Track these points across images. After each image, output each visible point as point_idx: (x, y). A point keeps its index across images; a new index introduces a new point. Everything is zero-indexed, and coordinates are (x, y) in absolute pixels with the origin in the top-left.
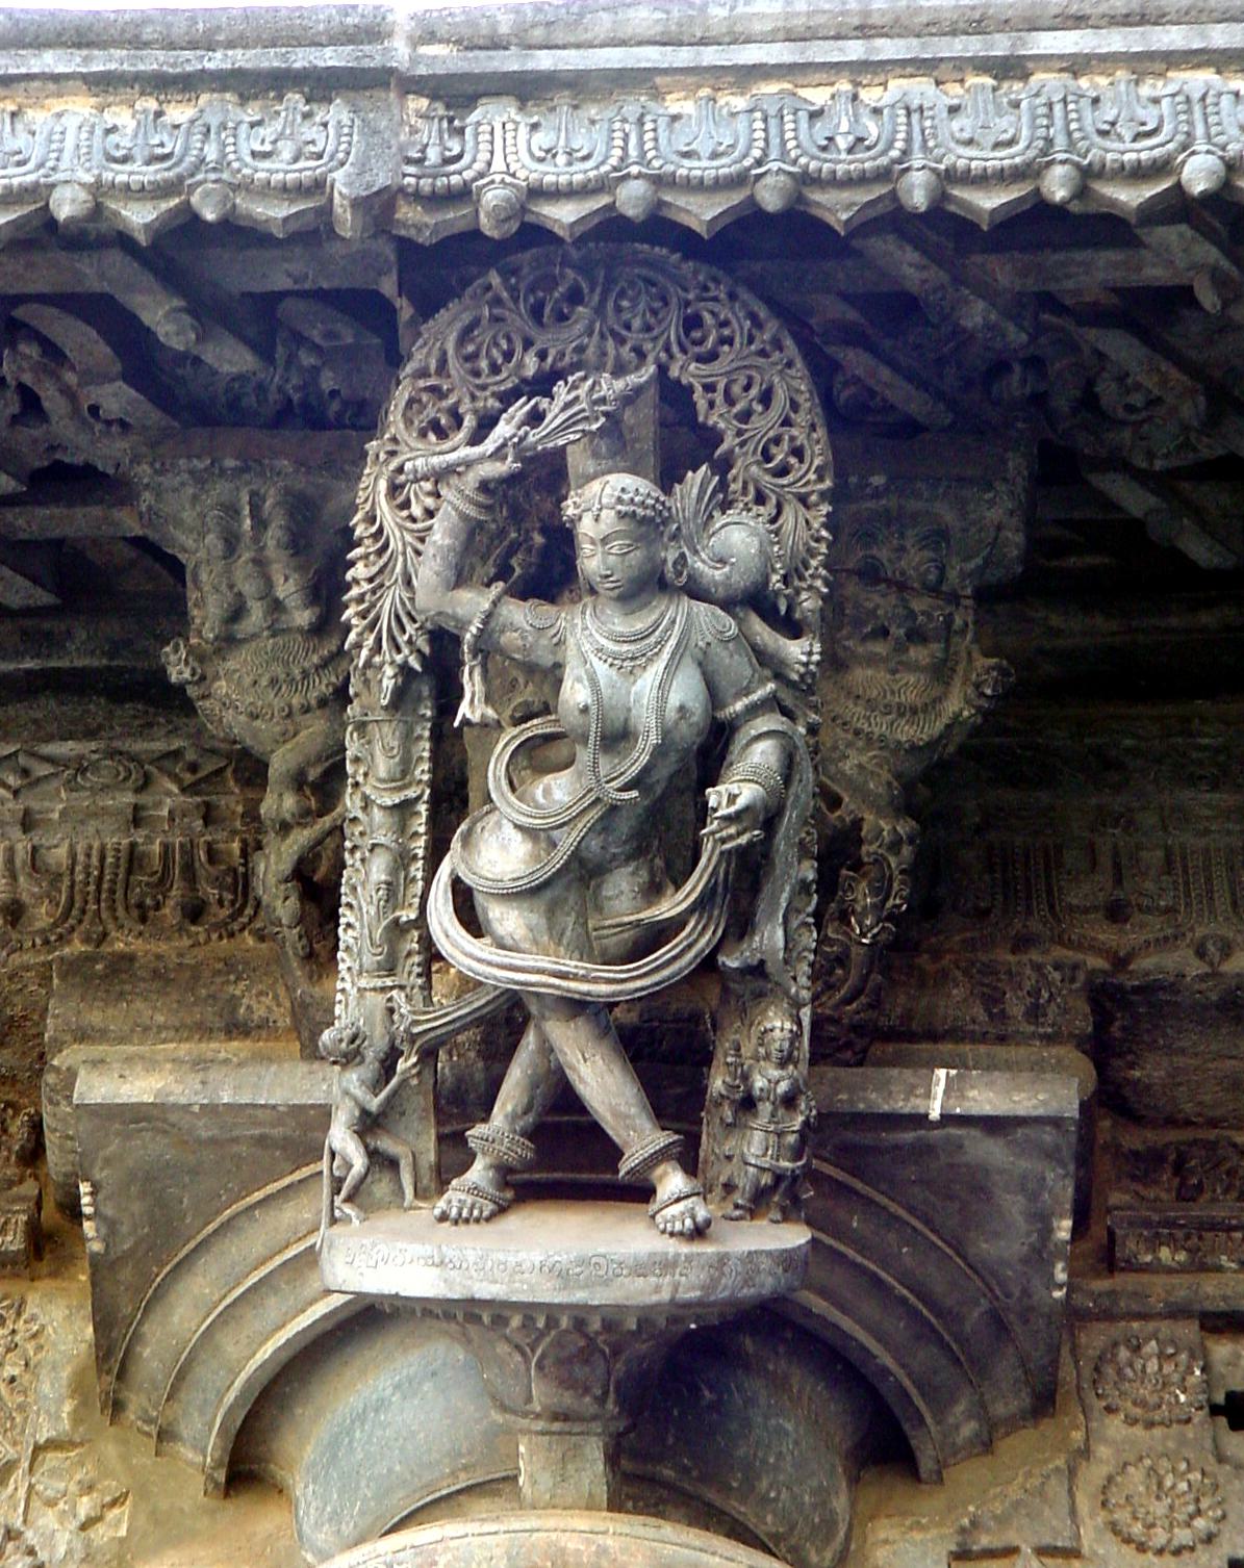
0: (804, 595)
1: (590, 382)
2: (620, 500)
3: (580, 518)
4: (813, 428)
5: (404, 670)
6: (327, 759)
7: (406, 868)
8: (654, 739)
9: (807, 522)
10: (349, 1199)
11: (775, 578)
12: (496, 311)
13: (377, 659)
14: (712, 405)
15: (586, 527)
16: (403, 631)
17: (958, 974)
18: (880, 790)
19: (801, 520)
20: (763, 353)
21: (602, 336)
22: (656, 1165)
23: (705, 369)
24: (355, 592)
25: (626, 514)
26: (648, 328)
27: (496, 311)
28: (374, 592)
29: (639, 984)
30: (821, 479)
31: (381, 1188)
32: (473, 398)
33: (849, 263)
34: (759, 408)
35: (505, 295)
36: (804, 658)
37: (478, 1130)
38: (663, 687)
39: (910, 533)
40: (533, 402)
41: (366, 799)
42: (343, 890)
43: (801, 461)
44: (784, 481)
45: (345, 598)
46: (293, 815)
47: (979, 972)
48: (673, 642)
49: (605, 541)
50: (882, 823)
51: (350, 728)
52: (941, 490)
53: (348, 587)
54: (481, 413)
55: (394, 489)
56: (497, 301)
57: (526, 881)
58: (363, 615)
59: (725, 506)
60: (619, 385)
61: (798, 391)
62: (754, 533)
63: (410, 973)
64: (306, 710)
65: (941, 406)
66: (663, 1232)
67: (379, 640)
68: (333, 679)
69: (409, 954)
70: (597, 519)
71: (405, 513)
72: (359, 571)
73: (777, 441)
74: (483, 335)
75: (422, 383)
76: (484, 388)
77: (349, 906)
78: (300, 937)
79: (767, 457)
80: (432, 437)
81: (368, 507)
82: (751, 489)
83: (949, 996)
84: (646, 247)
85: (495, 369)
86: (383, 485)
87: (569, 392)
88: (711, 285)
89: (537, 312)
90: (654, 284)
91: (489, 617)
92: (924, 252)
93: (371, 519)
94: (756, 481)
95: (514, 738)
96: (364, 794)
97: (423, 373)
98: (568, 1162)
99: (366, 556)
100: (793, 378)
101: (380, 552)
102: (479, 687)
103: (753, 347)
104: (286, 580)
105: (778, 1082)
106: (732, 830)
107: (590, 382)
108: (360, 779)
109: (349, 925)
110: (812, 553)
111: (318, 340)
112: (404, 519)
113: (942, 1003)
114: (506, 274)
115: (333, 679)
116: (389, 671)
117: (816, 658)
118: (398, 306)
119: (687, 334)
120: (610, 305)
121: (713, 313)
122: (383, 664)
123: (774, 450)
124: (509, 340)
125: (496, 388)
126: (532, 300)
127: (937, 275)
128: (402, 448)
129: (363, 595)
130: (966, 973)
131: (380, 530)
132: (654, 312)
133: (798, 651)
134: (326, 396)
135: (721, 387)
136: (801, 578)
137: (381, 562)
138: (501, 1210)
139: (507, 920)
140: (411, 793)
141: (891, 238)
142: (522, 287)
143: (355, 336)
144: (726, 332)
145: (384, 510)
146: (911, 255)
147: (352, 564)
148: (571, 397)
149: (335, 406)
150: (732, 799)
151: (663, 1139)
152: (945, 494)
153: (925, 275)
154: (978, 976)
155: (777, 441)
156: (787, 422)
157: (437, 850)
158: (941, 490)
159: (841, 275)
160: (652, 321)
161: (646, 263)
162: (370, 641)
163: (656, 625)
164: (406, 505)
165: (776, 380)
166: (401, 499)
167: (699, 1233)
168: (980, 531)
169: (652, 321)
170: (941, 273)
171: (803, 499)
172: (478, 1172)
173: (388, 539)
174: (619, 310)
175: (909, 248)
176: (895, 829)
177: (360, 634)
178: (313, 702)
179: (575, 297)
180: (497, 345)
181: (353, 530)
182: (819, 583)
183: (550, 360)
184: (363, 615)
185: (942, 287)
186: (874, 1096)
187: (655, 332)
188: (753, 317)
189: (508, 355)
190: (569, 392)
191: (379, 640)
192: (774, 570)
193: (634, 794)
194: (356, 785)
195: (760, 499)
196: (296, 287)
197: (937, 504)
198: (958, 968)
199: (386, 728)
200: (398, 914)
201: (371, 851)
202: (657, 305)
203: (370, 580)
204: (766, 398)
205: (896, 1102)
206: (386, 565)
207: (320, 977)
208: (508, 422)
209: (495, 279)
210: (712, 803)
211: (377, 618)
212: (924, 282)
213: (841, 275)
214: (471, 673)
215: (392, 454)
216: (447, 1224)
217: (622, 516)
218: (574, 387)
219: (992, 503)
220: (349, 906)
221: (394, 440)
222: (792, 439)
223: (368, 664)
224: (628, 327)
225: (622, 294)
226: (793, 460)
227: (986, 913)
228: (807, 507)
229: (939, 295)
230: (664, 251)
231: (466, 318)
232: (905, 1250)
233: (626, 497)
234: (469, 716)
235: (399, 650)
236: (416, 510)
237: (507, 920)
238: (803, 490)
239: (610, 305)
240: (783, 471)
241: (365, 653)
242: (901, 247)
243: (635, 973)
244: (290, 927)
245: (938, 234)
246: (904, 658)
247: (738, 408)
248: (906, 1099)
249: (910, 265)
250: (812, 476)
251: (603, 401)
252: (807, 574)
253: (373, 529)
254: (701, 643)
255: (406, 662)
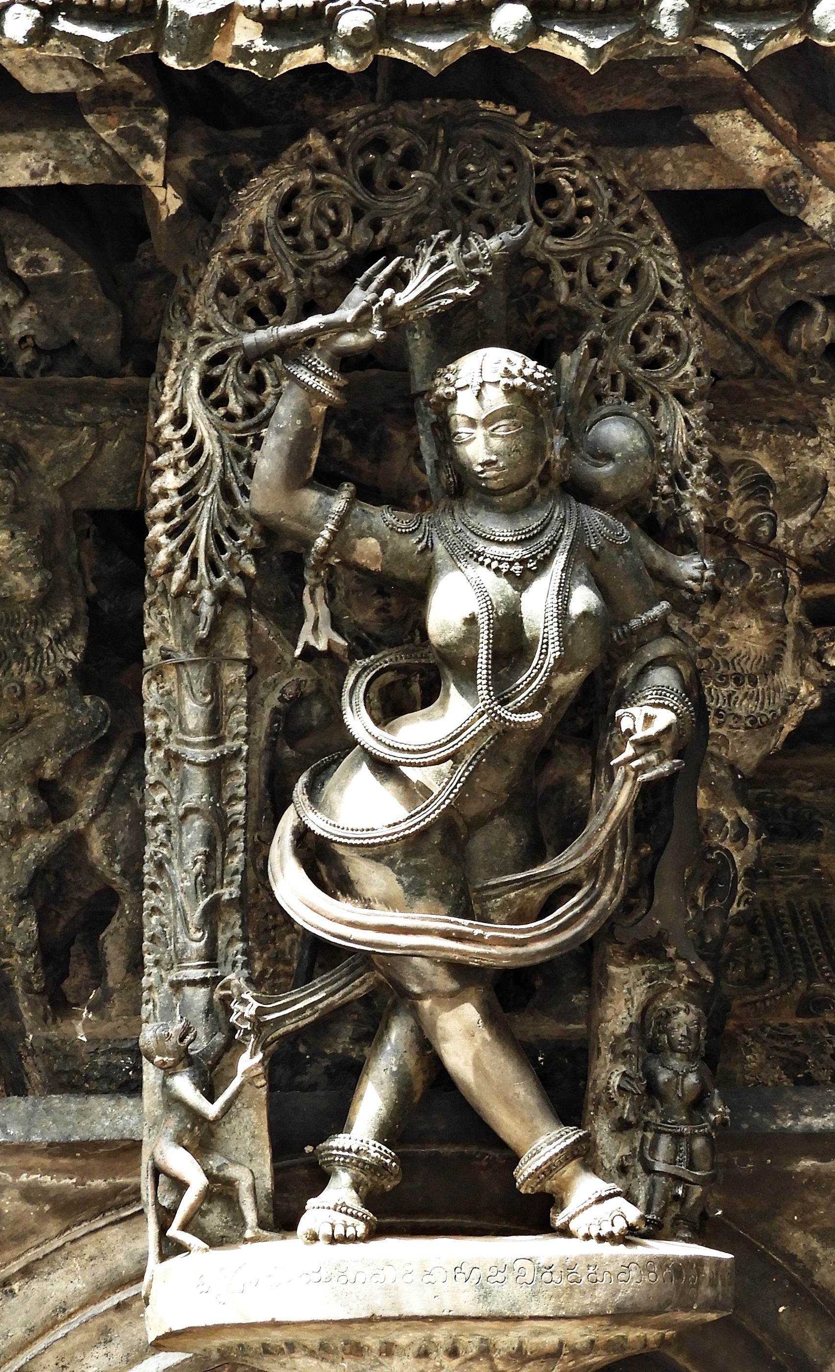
0: (687, 505)
1: (458, 240)
2: (508, 373)
3: (454, 398)
4: (686, 313)
5: (223, 596)
6: (69, 747)
7: (225, 835)
8: (554, 651)
9: (686, 420)
10: (184, 1227)
11: (663, 478)
12: (321, 177)
13: (194, 585)
14: (572, 285)
15: (465, 406)
16: (222, 549)
17: (748, 1039)
18: (723, 773)
19: (680, 418)
20: (627, 227)
21: (445, 207)
22: (567, 1161)
23: (567, 244)
24: (163, 505)
25: (514, 388)
26: (495, 197)
27: (321, 177)
28: (186, 505)
29: (541, 945)
30: (699, 373)
31: (215, 1220)
32: (297, 274)
33: (680, 151)
34: (628, 289)
35: (330, 157)
36: (696, 573)
37: (340, 1141)
38: (564, 594)
39: (733, 480)
40: (393, 263)
41: (174, 759)
42: (146, 869)
43: (677, 352)
44: (660, 373)
45: (153, 512)
46: (30, 815)
47: (770, 1036)
48: (565, 544)
49: (488, 421)
50: (723, 811)
51: (147, 677)
52: (760, 436)
53: (155, 502)
54: (307, 294)
55: (208, 385)
56: (320, 166)
57: (404, 826)
58: (171, 534)
59: (600, 399)
60: (493, 243)
61: (669, 271)
62: (640, 424)
63: (234, 964)
64: (42, 688)
65: (738, 349)
66: (587, 1237)
67: (194, 562)
68: (71, 655)
69: (230, 942)
70: (479, 396)
71: (222, 411)
72: (170, 481)
73: (647, 328)
74: (306, 204)
75: (236, 260)
76: (306, 263)
77: (154, 887)
78: (35, 968)
79: (638, 345)
80: (250, 322)
81: (176, 405)
82: (622, 381)
83: (744, 1061)
84: (490, 106)
85: (322, 243)
86: (195, 378)
87: (433, 254)
88: (567, 148)
89: (366, 177)
90: (500, 147)
91: (343, 519)
92: (774, 134)
93: (179, 420)
94: (626, 371)
95: (365, 669)
96: (168, 752)
97: (235, 251)
98: (447, 1178)
99: (175, 466)
100: (663, 256)
101: (193, 459)
102: (323, 611)
103: (618, 221)
104: (13, 536)
105: (685, 1076)
106: (653, 757)
107: (458, 240)
108: (161, 735)
109: (154, 910)
110: (693, 459)
111: (20, 270)
112: (222, 418)
113: (738, 1068)
114: (330, 136)
115: (71, 655)
116: (207, 595)
117: (707, 574)
118: (160, 197)
119: (541, 206)
120: (453, 169)
121: (573, 182)
122: (200, 588)
123: (645, 338)
124: (337, 212)
125: (323, 263)
126: (361, 163)
127: (785, 158)
128: (216, 334)
129: (173, 508)
130: (755, 1037)
131: (192, 432)
132: (502, 177)
133: (689, 567)
134: (16, 342)
135: (585, 263)
136: (684, 487)
137: (194, 470)
138: (375, 1232)
139: (374, 878)
140: (231, 744)
141: (739, 113)
142: (347, 147)
143: (63, 266)
144: (588, 202)
145: (196, 409)
146: (761, 136)
147: (158, 472)
148: (437, 257)
149: (27, 356)
150: (648, 719)
151: (571, 1135)
152: (766, 440)
153: (773, 160)
154: (769, 1040)
155: (647, 328)
156: (659, 306)
157: (277, 801)
158: (760, 436)
159: (668, 167)
160: (501, 186)
161: (489, 122)
162: (185, 561)
163: (545, 526)
164: (223, 401)
165: (643, 255)
166: (214, 396)
167: (630, 1235)
168: (801, 486)
169: (501, 186)
170: (792, 159)
171: (679, 396)
172: (341, 1190)
173: (201, 444)
174: (463, 174)
175: (758, 127)
176: (739, 818)
177: (172, 555)
178: (51, 681)
179: (409, 160)
180: (322, 214)
181: (158, 431)
182: (702, 492)
183: (384, 233)
184: (171, 534)
185: (794, 174)
186: (757, 1115)
187: (504, 202)
188: (612, 183)
189: (336, 227)
190: (433, 254)
191: (194, 562)
192: (662, 471)
193: (536, 716)
194: (157, 744)
195: (632, 394)
196: (34, 182)
197: (756, 453)
198: (746, 1033)
199: (193, 672)
200: (216, 892)
201: (183, 818)
202: (507, 170)
203: (181, 491)
204: (633, 276)
205: (784, 1120)
206: (200, 472)
207: (54, 1021)
208: (365, 287)
209: (315, 140)
210: (626, 724)
211: (191, 536)
212: (771, 169)
213: (668, 167)
214: (312, 594)
215: (203, 342)
216: (322, 1244)
217: (509, 391)
218: (439, 247)
219: (818, 450)
220: (154, 887)
221: (206, 327)
222: (666, 327)
223: (182, 592)
224: (471, 193)
225: (466, 157)
226: (668, 350)
227: (765, 976)
228: (686, 404)
229: (791, 183)
230: (512, 110)
231: (287, 184)
232: (781, 1309)
233: (514, 371)
234: (312, 642)
235: (218, 575)
236: (235, 406)
237: (374, 878)
238: (681, 385)
239: (453, 169)
240: (655, 362)
241: (178, 575)
242: (747, 126)
243: (546, 930)
244: (22, 954)
245: (784, 118)
246: (736, 623)
247: (605, 288)
248: (795, 1118)
249: (759, 148)
250: (688, 368)
251: (474, 262)
252: (689, 481)
253: (184, 431)
254: (594, 546)
255: (225, 583)
